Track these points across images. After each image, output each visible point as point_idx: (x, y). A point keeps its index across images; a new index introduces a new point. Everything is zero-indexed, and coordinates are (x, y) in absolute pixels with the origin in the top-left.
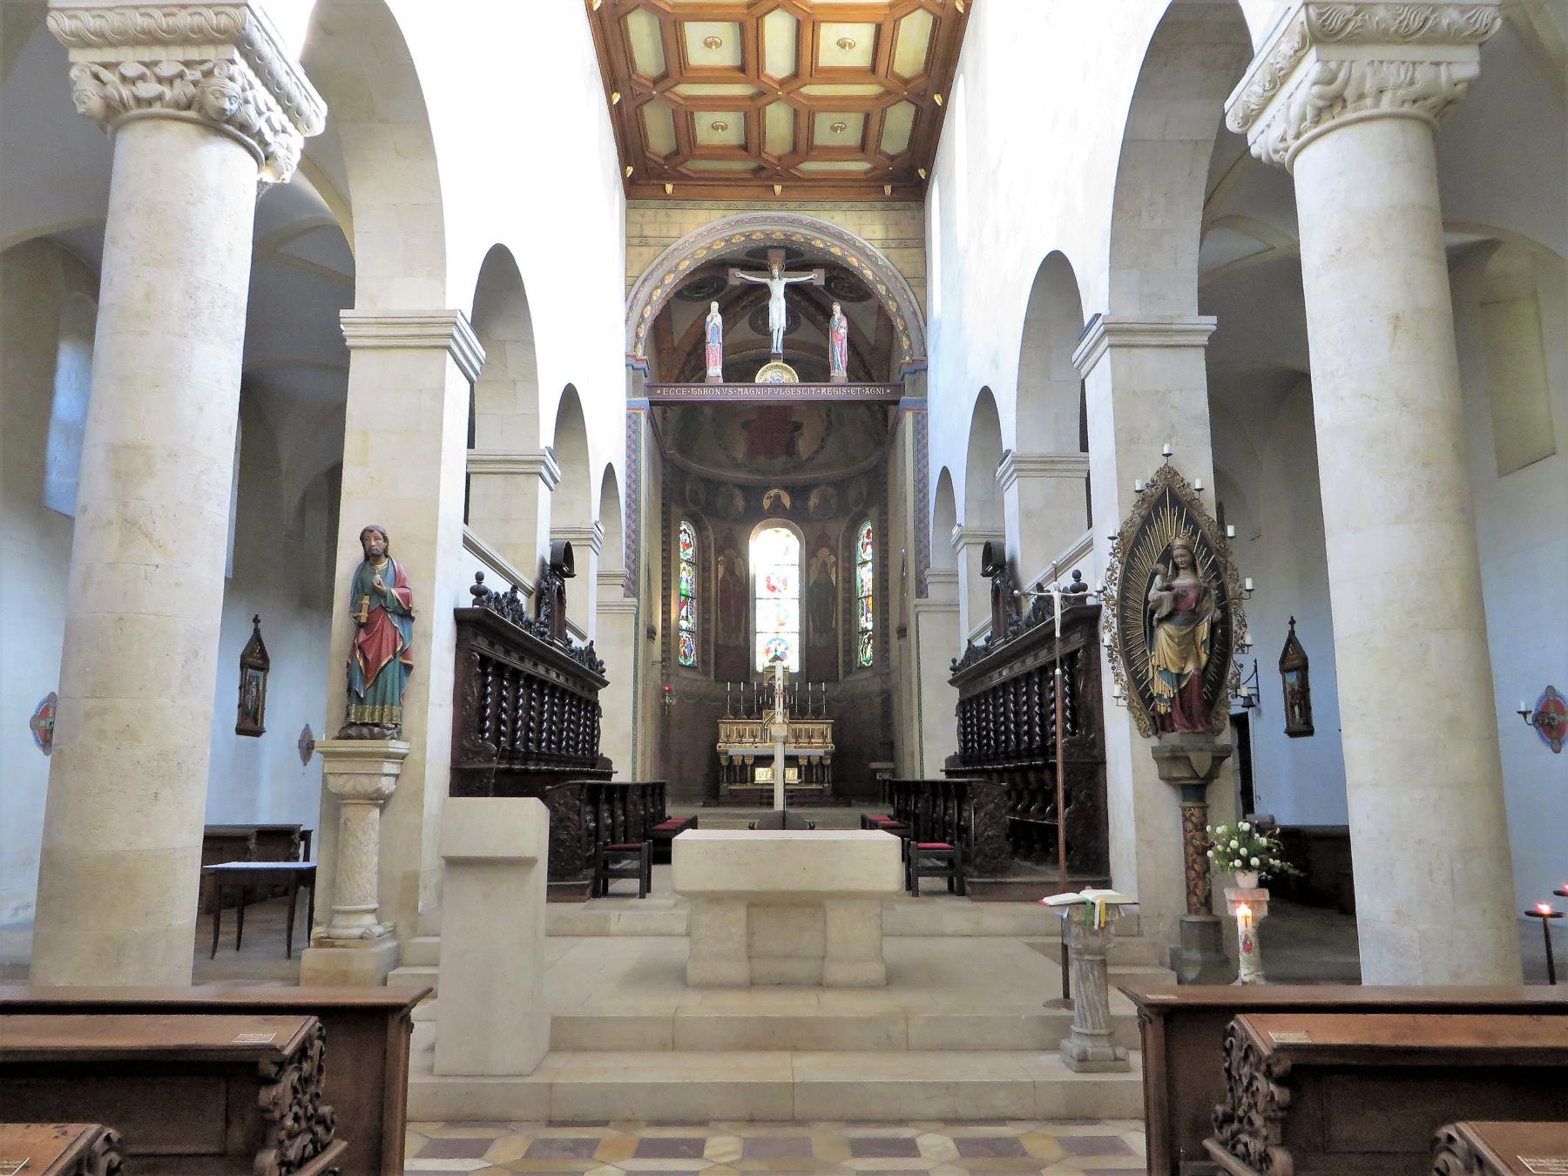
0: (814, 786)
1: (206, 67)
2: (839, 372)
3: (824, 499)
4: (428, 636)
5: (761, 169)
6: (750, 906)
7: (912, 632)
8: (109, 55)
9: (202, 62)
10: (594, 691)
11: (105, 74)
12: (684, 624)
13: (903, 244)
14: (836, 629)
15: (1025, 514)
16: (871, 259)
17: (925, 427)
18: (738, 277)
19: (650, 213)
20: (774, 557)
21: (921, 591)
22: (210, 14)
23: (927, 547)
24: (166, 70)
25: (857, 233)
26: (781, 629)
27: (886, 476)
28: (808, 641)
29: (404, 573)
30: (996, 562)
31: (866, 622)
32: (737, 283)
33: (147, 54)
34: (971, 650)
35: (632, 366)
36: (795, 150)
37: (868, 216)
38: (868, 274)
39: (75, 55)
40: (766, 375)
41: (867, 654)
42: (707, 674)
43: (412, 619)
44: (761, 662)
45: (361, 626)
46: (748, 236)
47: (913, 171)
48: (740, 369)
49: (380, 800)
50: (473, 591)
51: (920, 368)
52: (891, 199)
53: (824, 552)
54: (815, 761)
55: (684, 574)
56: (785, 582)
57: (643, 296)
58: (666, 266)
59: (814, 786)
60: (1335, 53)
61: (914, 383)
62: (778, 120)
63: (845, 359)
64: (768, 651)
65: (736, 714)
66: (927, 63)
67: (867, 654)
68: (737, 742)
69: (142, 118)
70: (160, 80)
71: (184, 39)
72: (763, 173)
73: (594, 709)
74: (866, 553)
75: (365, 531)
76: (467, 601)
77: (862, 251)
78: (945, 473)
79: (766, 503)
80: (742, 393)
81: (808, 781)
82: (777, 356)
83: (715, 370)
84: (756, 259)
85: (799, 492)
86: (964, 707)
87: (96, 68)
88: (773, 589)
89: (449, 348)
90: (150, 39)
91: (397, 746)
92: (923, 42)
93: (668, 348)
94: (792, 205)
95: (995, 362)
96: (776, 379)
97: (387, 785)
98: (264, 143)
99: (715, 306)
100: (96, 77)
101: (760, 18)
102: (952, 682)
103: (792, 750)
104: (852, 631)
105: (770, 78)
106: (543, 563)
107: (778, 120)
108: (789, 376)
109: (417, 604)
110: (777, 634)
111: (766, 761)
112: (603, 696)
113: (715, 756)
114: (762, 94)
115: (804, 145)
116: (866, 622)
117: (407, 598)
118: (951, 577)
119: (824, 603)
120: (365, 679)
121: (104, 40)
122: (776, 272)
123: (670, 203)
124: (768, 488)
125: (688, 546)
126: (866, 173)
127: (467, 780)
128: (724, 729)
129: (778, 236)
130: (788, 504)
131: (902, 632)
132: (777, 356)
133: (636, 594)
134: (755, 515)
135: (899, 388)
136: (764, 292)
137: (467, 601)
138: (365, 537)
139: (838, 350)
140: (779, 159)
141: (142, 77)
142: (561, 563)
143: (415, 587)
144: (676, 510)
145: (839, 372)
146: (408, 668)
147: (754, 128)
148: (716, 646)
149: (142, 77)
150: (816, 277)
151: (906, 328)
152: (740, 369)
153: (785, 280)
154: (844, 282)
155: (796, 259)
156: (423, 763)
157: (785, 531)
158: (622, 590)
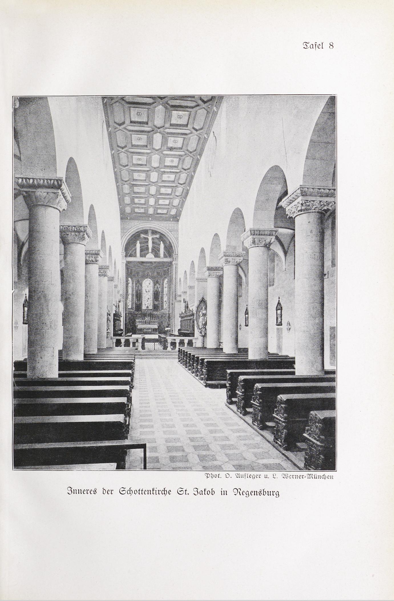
18: (142, 236)
40: (147, 256)
53: (158, 285)
60: (210, 271)
84: (146, 232)
96: (150, 257)
107: (151, 211)
150: (158, 236)
154: (162, 237)
155: (154, 232)
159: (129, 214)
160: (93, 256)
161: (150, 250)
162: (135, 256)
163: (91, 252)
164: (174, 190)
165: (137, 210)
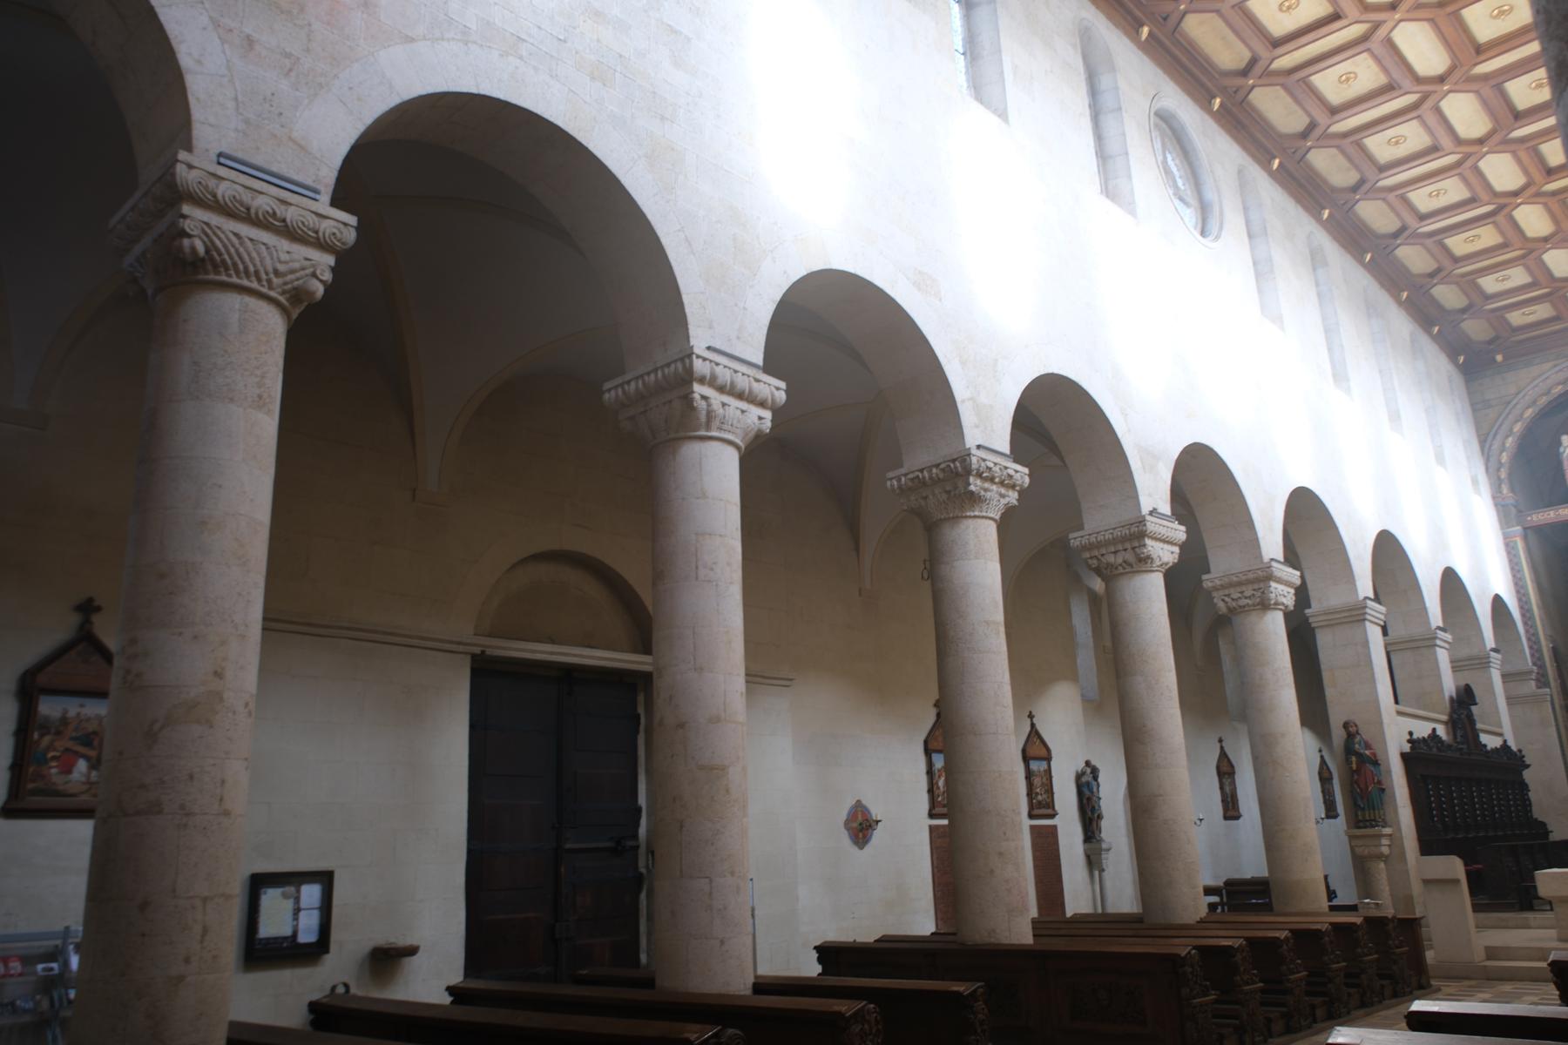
4: (1389, 772)
24: (1248, 593)
39: (1215, 594)
49: (1380, 857)
57: (1496, 446)
73: (1523, 787)
76: (1407, 748)
90: (1240, 584)
97: (1385, 850)
106: (1451, 699)
109: (1380, 756)
112: (1527, 774)
121: (1223, 587)
127: (1429, 846)
133: (1547, 685)
137: (1407, 748)
138: (1346, 725)
142: (1465, 699)
146: (1383, 790)
156: (1401, 838)
158: (1533, 683)
159: (1490, 342)
160: (1128, 545)
163: (1118, 533)
165: (1516, 318)
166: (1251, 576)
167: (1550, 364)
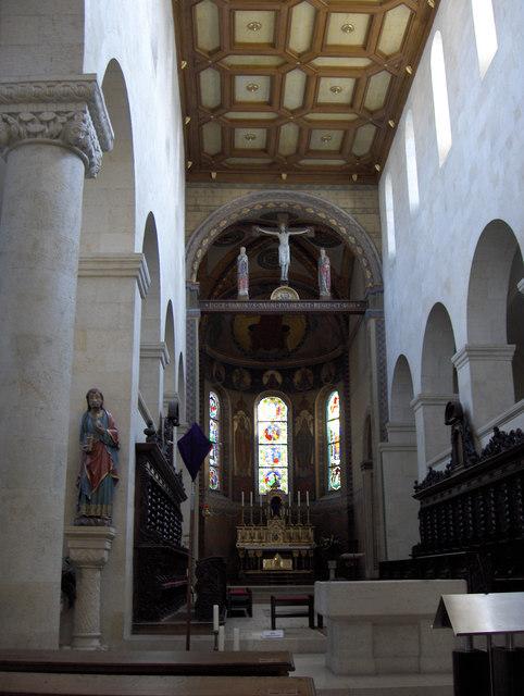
0: (304, 571)
1: (70, 115)
2: (326, 292)
3: (305, 378)
5: (274, 163)
6: (374, 625)
7: (376, 464)
8: (13, 108)
9: (67, 113)
10: (180, 502)
11: (10, 119)
12: (212, 462)
13: (365, 211)
14: (313, 465)
15: (475, 384)
16: (346, 220)
17: (383, 329)
19: (201, 191)
20: (270, 414)
21: (384, 438)
22: (74, 86)
23: (386, 408)
24: (47, 116)
25: (334, 204)
26: (276, 465)
27: (348, 362)
28: (294, 474)
29: (113, 420)
30: (455, 414)
31: (335, 460)
32: (258, 235)
33: (33, 107)
34: (432, 475)
35: (189, 289)
36: (298, 151)
37: (342, 194)
38: (343, 230)
40: (278, 294)
41: (335, 482)
42: (227, 496)
43: (118, 449)
44: (264, 487)
45: (88, 453)
46: (265, 206)
47: (371, 166)
48: (262, 288)
50: (146, 432)
51: (379, 290)
52: (355, 183)
53: (305, 413)
54: (304, 554)
55: (212, 428)
56: (278, 434)
58: (212, 224)
59: (304, 571)
61: (374, 299)
62: (289, 134)
63: (329, 284)
64: (267, 480)
65: (247, 522)
66: (386, 101)
67: (335, 482)
68: (249, 540)
69: (30, 143)
70: (42, 122)
71: (60, 99)
72: (274, 166)
74: (334, 409)
75: (90, 391)
76: (143, 439)
77: (339, 215)
78: (402, 360)
79: (265, 380)
80: (263, 306)
81: (299, 569)
82: (284, 283)
83: (244, 291)
84: (269, 219)
85: (288, 373)
86: (423, 514)
87: (5, 116)
88: (269, 437)
89: (137, 277)
91: (113, 531)
92: (384, 90)
93: (210, 279)
94: (293, 186)
95: (447, 286)
97: (105, 554)
98: (91, 157)
99: (243, 249)
100: (5, 120)
101: (284, 75)
102: (415, 497)
103: (286, 546)
104: (325, 467)
105: (287, 109)
107: (289, 134)
108: (293, 295)
109: (121, 440)
110: (273, 466)
111: (269, 554)
113: (234, 550)
114: (280, 118)
115: (304, 149)
116: (335, 460)
117: (116, 435)
118: (412, 428)
119: (304, 445)
120: (92, 488)
122: (283, 228)
123: (214, 185)
124: (266, 370)
125: (214, 409)
126: (341, 166)
128: (241, 532)
129: (284, 205)
130: (279, 379)
131: (368, 466)
132: (284, 283)
134: (260, 389)
135: (365, 303)
136: (277, 241)
137: (143, 439)
139: (324, 278)
140: (286, 157)
141: (32, 121)
143: (120, 428)
144: (207, 384)
145: (326, 292)
147: (273, 139)
148: (233, 476)
149: (32, 121)
151: (368, 265)
152: (262, 288)
153: (289, 233)
154: (328, 236)
155: (295, 222)
157: (277, 399)
161: (285, 271)
162: (232, 293)
164: (378, 20)
166: (59, 89)
167: (247, 191)
